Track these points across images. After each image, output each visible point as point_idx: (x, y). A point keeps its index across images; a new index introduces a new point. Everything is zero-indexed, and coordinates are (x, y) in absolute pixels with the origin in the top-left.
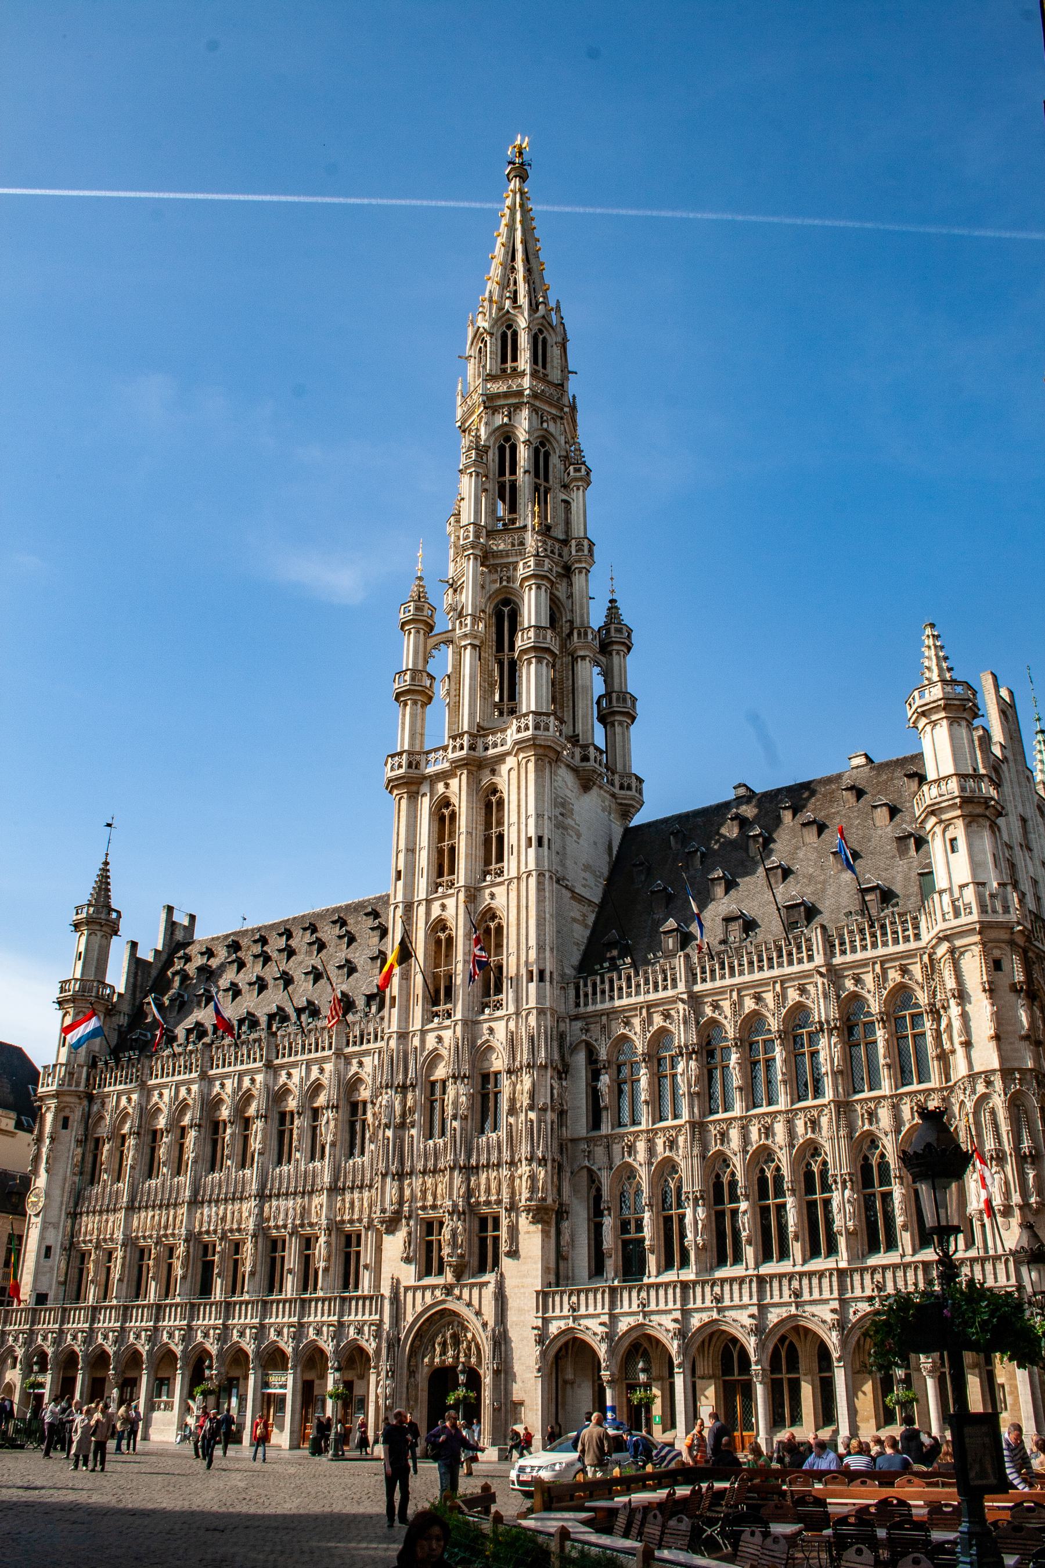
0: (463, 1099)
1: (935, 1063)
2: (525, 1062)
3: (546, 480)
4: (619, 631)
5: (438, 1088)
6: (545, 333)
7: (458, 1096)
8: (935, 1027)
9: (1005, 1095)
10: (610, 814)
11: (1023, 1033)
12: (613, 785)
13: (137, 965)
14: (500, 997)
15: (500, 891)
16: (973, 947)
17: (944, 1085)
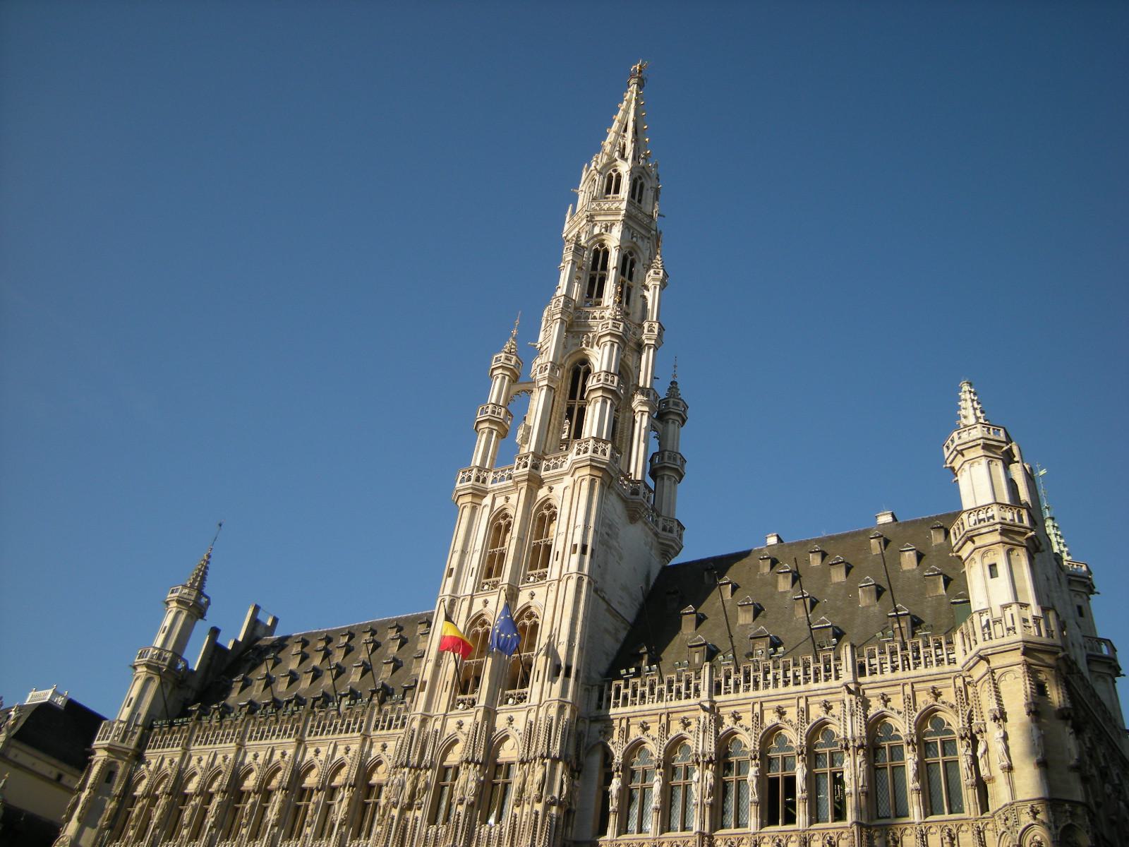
0: (472, 785)
1: (970, 791)
2: (539, 753)
3: (630, 278)
4: (676, 404)
5: (451, 772)
6: (643, 180)
7: (468, 781)
8: (970, 752)
9: (1057, 828)
10: (651, 549)
11: (1072, 762)
12: (657, 525)
13: (215, 650)
14: (525, 690)
15: (540, 591)
16: (1015, 667)
17: (979, 816)
